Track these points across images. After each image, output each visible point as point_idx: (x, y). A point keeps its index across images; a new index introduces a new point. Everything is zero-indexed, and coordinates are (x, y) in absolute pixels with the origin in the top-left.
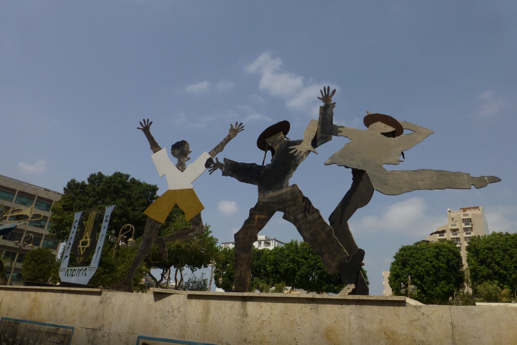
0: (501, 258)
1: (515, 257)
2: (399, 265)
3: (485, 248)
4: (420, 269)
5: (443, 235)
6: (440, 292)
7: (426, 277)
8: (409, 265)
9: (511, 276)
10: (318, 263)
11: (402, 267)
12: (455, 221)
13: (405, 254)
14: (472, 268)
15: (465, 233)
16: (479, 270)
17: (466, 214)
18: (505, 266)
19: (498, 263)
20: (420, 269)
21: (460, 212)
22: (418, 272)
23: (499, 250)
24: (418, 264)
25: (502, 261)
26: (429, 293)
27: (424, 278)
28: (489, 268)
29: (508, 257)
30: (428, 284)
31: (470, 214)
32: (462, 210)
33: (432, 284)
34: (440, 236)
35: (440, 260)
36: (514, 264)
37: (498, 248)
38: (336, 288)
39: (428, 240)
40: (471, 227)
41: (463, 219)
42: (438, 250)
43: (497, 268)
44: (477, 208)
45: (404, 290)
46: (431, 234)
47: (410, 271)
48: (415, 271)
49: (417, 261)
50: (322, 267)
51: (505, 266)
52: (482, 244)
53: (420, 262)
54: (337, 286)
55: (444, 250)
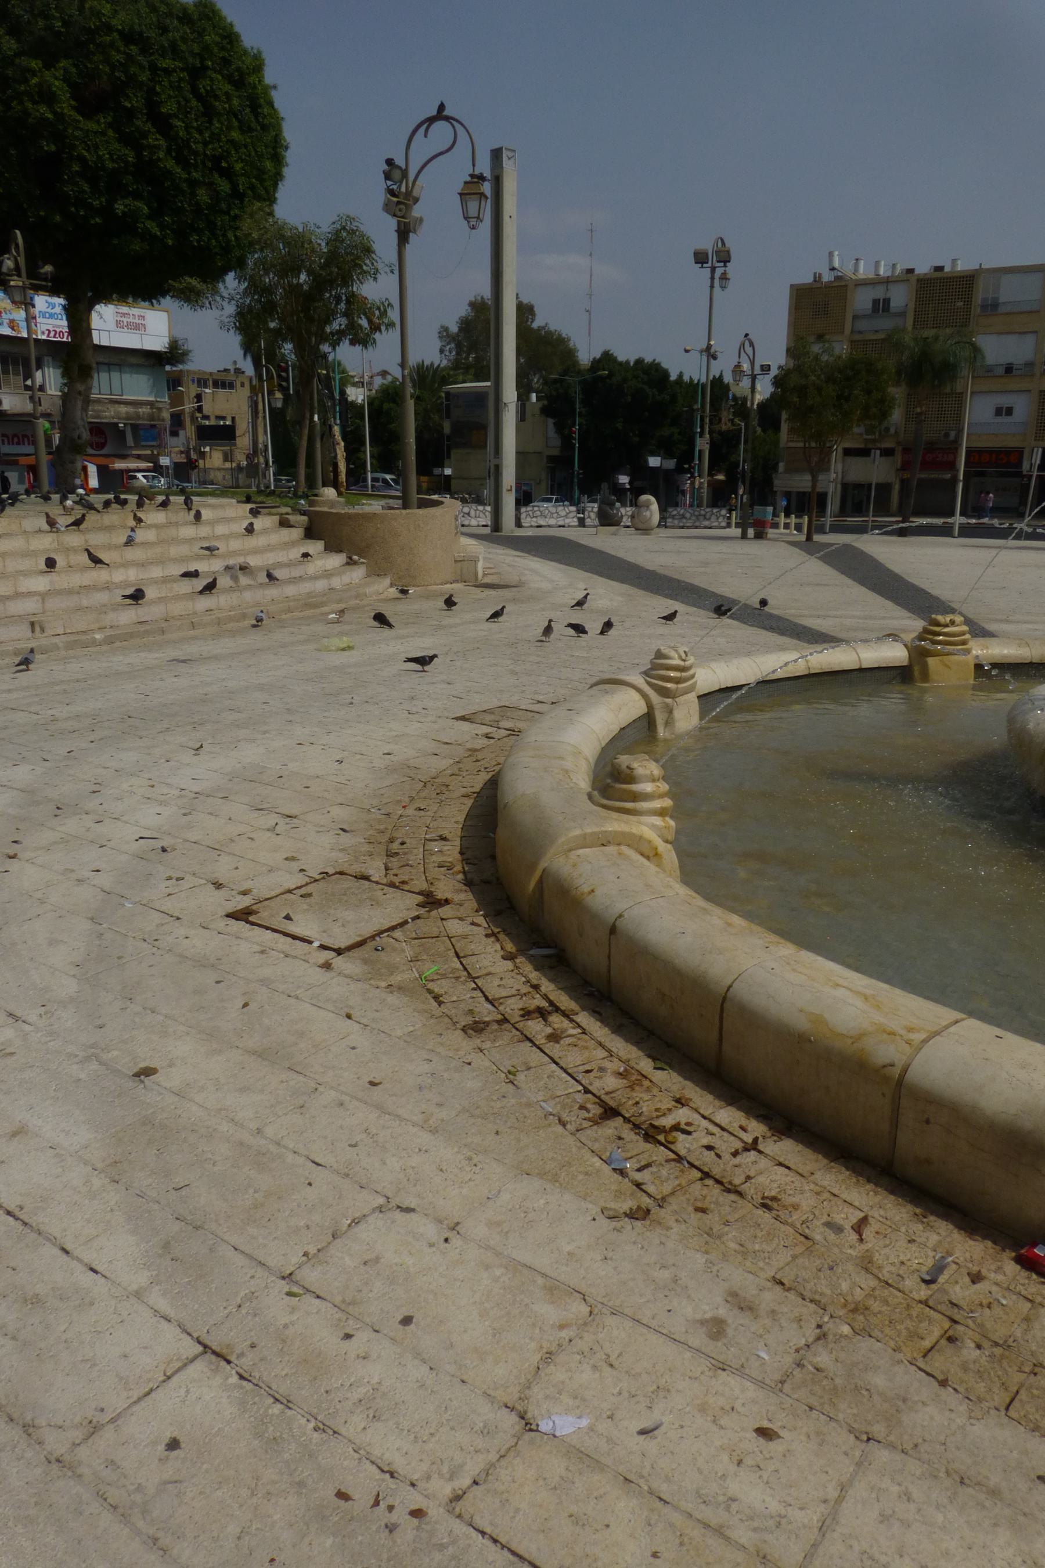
9: (193, 194)
19: (163, 124)
28: (126, 140)
43: (158, 147)
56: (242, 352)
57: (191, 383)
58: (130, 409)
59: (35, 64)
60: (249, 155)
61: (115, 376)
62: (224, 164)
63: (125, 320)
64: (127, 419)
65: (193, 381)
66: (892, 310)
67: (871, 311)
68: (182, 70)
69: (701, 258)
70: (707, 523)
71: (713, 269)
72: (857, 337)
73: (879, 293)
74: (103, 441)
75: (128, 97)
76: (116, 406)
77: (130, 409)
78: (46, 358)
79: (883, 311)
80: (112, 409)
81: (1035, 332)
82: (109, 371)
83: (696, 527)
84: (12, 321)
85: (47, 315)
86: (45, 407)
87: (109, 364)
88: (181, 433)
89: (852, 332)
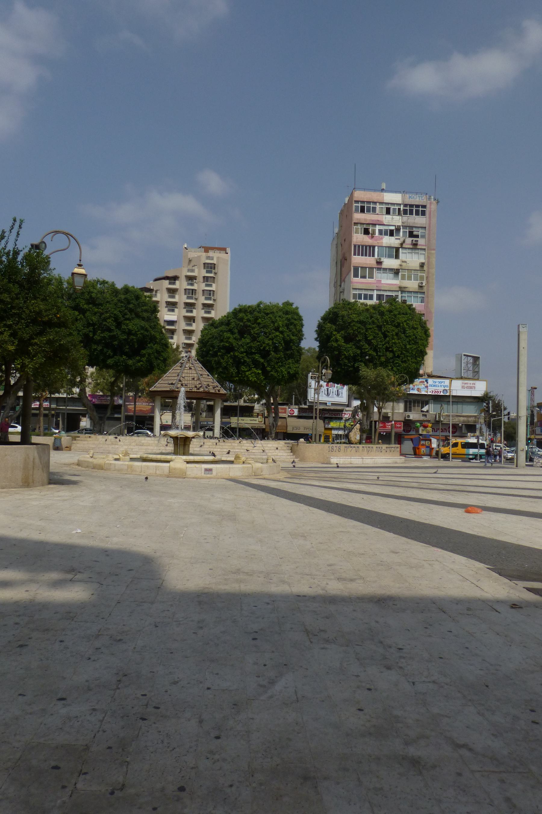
0: (374, 337)
1: (389, 336)
2: (236, 333)
3: (357, 321)
4: (267, 341)
5: (174, 284)
6: (285, 374)
8: (250, 334)
9: (379, 359)
10: (105, 320)
11: (239, 337)
12: (192, 264)
13: (246, 318)
14: (336, 345)
15: (204, 284)
17: (209, 257)
19: (369, 343)
20: (267, 341)
21: (201, 252)
22: (262, 347)
23: (374, 326)
25: (373, 339)
26: (272, 375)
27: (269, 355)
28: (358, 348)
29: (382, 336)
31: (215, 257)
32: (203, 250)
33: (277, 363)
34: (170, 284)
35: (290, 331)
36: (387, 344)
37: (373, 322)
38: (130, 362)
39: (152, 288)
40: (213, 277)
41: (204, 264)
42: (289, 316)
44: (224, 249)
46: (156, 280)
47: (250, 342)
50: (113, 328)
52: (354, 315)
54: (131, 359)
55: (296, 317)
58: (465, 419)
60: (400, 346)
61: (460, 406)
62: (390, 349)
63: (466, 386)
64: (463, 422)
68: (375, 327)
74: (455, 430)
76: (459, 417)
77: (465, 419)
78: (431, 401)
80: (457, 419)
82: (457, 404)
84: (418, 388)
85: (433, 386)
86: (428, 418)
87: (457, 402)
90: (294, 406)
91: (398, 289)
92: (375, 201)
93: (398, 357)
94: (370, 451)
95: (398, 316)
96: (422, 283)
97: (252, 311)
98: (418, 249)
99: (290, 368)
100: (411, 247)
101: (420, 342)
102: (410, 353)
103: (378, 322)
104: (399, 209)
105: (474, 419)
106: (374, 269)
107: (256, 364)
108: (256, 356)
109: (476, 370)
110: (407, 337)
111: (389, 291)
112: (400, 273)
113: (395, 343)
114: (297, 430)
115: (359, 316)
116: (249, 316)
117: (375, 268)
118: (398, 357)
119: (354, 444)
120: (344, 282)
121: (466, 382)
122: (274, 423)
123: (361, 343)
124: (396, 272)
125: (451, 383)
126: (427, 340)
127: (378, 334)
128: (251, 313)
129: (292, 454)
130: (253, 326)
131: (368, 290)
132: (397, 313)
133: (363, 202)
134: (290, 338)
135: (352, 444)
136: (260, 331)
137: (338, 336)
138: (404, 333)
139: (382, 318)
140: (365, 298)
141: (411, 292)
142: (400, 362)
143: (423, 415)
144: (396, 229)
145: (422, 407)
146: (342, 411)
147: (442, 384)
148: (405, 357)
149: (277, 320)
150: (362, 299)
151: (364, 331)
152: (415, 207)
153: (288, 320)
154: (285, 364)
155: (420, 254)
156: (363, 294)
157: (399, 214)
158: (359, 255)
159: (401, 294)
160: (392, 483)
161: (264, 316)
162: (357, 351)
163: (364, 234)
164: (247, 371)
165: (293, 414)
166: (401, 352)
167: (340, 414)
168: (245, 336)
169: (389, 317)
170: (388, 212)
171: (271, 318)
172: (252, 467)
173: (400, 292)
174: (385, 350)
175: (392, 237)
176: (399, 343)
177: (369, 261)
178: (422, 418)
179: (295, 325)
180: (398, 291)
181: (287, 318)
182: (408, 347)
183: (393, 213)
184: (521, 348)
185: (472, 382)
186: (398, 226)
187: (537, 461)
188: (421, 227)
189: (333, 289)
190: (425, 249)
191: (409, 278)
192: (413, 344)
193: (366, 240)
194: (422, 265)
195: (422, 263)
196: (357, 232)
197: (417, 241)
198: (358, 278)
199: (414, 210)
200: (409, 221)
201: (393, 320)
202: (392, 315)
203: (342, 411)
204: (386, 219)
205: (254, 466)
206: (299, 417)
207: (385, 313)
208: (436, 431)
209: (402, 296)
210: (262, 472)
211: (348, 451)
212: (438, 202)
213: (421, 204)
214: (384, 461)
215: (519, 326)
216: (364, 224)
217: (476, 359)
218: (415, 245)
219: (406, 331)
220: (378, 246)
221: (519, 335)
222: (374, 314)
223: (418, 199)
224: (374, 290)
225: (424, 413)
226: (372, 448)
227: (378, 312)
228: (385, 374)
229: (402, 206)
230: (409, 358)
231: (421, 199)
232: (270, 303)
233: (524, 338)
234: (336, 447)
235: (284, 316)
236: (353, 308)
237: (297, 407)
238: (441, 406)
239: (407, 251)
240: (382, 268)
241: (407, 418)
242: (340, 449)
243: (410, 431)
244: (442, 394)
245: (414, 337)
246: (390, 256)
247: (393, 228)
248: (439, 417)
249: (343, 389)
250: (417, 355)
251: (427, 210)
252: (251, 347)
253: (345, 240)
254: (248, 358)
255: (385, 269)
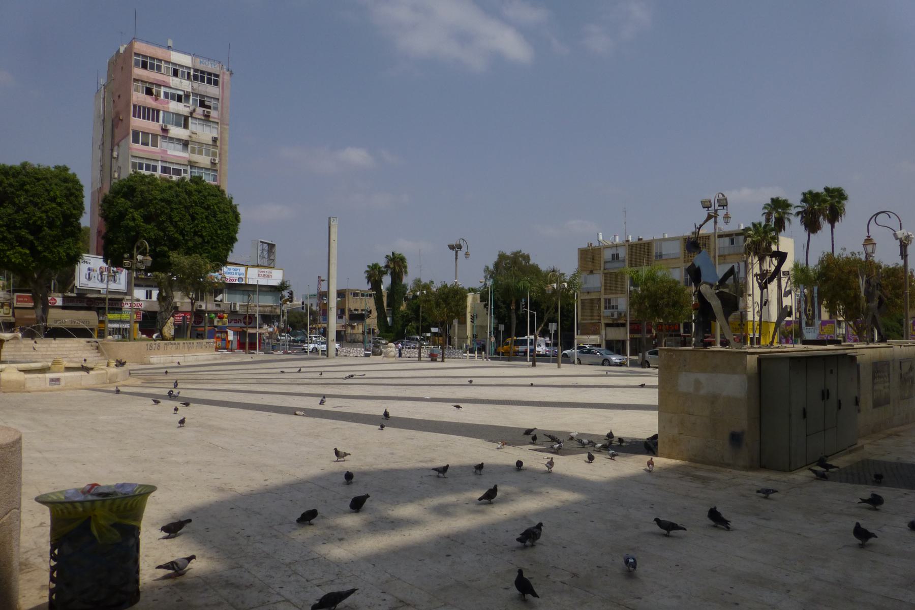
0: (180, 218)
1: (198, 219)
6: (63, 256)
7: (45, 228)
8: (14, 204)
14: (133, 225)
16: (144, 229)
18: (184, 229)
20: (38, 214)
22: (30, 220)
24: (36, 204)
26: (44, 256)
28: (160, 229)
30: (46, 241)
33: (53, 242)
35: (71, 203)
37: (180, 203)
43: (172, 231)
45: (129, 262)
47: (13, 213)
48: (26, 216)
49: (31, 198)
51: (184, 229)
52: (157, 192)
53: (39, 201)
56: (366, 281)
57: (350, 294)
59: (131, 210)
63: (262, 274)
65: (351, 294)
66: (620, 259)
67: (611, 260)
68: (182, 208)
69: (452, 247)
70: (453, 356)
71: (457, 252)
72: (606, 271)
73: (614, 251)
75: (161, 217)
79: (616, 259)
81: (679, 267)
83: (449, 358)
86: (222, 308)
88: (344, 317)
89: (605, 269)
90: (56, 294)
91: (187, 163)
92: (160, 58)
93: (208, 242)
94: (190, 348)
95: (207, 198)
96: (214, 160)
97: (16, 173)
98: (211, 121)
99: (69, 248)
100: (203, 118)
101: (231, 228)
102: (220, 239)
103: (186, 202)
104: (189, 74)
105: (270, 309)
106: (159, 137)
107: (22, 242)
108: (23, 231)
109: (272, 257)
110: (218, 221)
111: (176, 163)
112: (189, 146)
113: (204, 227)
114: (62, 324)
115: (162, 193)
116: (12, 180)
117: (160, 135)
118: (208, 242)
119: (168, 340)
120: (118, 146)
121: (263, 270)
122: (44, 316)
123: (165, 224)
124: (185, 144)
125: (246, 271)
126: (237, 225)
127: (185, 216)
128: (14, 176)
129: (99, 354)
130: (17, 192)
131: (151, 159)
132: (207, 194)
133: (146, 57)
134: (70, 211)
135: (167, 340)
136: (28, 200)
137: (136, 215)
138: (215, 217)
139: (190, 198)
140: (148, 168)
141: (202, 168)
142: (210, 248)
143: (217, 305)
144: (185, 95)
145: (216, 296)
146: (121, 300)
147: (237, 272)
148: (215, 243)
149: (52, 188)
150: (143, 170)
151: (169, 210)
152: (207, 75)
153: (69, 190)
154: (63, 243)
155: (213, 127)
156: (144, 164)
157: (189, 78)
158: (139, 117)
159: (191, 169)
160: (264, 381)
161: (34, 182)
162: (160, 233)
163: (146, 94)
164: (9, 250)
165: (55, 303)
166: (212, 237)
167: (118, 303)
168: (6, 205)
169: (198, 198)
170: (175, 73)
171: (44, 185)
172: (107, 373)
173: (189, 167)
174: (192, 234)
175: (181, 104)
176: (209, 227)
177: (152, 126)
178: (215, 308)
179: (76, 197)
180: (187, 165)
181: (67, 187)
182: (219, 232)
183: (182, 76)
184: (332, 241)
185: (268, 270)
186: (187, 92)
187: (341, 350)
188: (214, 98)
189: (99, 153)
190: (218, 123)
191: (200, 153)
192: (224, 229)
193: (149, 101)
194: (215, 140)
195: (215, 137)
196: (137, 90)
197: (209, 112)
198: (139, 143)
199: (206, 78)
200: (200, 88)
201: (202, 201)
202: (201, 195)
203: (121, 300)
204: (174, 81)
205: (108, 372)
206: (63, 308)
207: (194, 193)
208: (231, 322)
209: (191, 172)
210: (117, 378)
211: (168, 348)
212: (231, 74)
213: (213, 72)
214: (206, 357)
215: (330, 218)
216: (146, 82)
217: (271, 246)
218: (207, 117)
219: (217, 214)
220: (163, 111)
221: (329, 227)
222: (180, 192)
223: (210, 66)
224: (158, 161)
225: (218, 303)
226: (193, 343)
227: (186, 191)
228: (202, 263)
229: (192, 70)
230: (219, 244)
231: (213, 66)
232: (39, 166)
233: (334, 230)
234: (155, 344)
235: (62, 184)
236: (154, 184)
237: (60, 295)
238: (249, 297)
239: (197, 122)
240: (167, 137)
241: (198, 308)
242: (159, 346)
243: (201, 322)
244: (237, 282)
245: (226, 222)
246: (178, 124)
247: (181, 93)
248: (235, 306)
249: (121, 273)
250: (227, 241)
251: (220, 80)
252: (14, 221)
253: (119, 96)
254: (10, 233)
255: (172, 139)
